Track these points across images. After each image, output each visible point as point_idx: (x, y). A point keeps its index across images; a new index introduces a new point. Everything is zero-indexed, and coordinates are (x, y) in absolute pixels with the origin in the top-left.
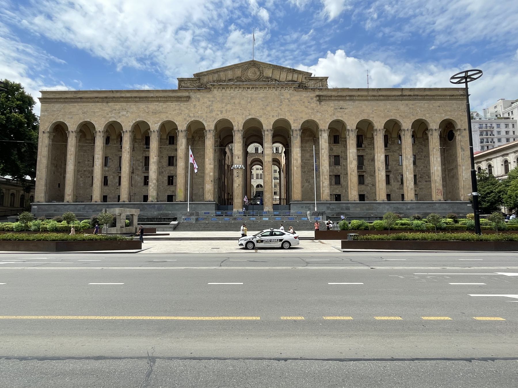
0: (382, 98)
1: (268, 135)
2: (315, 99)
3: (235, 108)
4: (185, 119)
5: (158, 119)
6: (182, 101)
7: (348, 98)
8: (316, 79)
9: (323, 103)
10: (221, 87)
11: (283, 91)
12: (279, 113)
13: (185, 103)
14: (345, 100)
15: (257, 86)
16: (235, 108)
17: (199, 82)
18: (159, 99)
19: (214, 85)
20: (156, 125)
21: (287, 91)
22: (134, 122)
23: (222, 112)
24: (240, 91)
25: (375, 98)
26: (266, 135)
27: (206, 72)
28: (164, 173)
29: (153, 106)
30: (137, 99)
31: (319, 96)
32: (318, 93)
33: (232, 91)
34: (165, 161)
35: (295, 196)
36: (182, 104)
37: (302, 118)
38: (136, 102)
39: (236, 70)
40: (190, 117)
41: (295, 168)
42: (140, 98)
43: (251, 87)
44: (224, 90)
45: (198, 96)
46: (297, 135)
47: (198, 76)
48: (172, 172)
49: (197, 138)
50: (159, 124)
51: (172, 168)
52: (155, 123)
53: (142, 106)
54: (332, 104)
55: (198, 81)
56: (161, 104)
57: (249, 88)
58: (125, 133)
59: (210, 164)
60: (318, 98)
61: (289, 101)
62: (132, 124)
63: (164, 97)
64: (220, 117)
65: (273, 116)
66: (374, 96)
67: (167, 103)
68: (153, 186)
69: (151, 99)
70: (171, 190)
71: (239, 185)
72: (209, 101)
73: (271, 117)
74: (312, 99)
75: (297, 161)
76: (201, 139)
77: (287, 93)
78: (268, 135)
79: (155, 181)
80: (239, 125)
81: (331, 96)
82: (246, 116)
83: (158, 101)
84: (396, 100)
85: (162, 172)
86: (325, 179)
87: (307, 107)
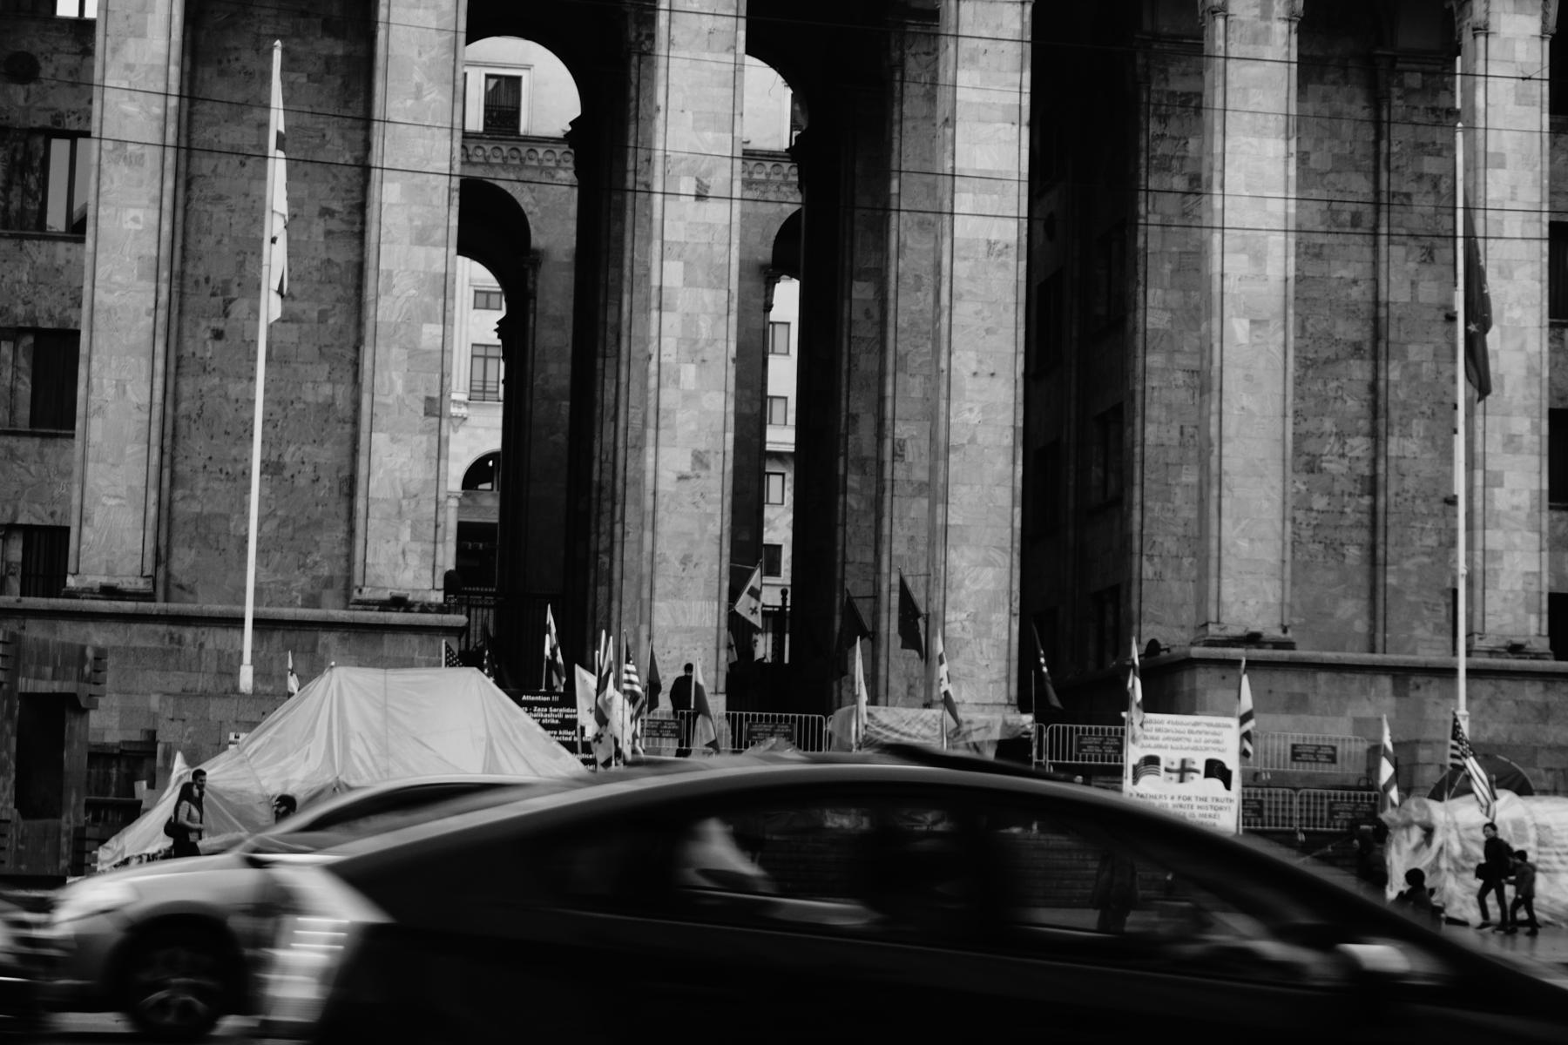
35: (1229, 591)
41: (1238, 329)
46: (1266, 15)
59: (422, 238)
71: (699, 459)
75: (1258, 258)
86: (1511, 443)
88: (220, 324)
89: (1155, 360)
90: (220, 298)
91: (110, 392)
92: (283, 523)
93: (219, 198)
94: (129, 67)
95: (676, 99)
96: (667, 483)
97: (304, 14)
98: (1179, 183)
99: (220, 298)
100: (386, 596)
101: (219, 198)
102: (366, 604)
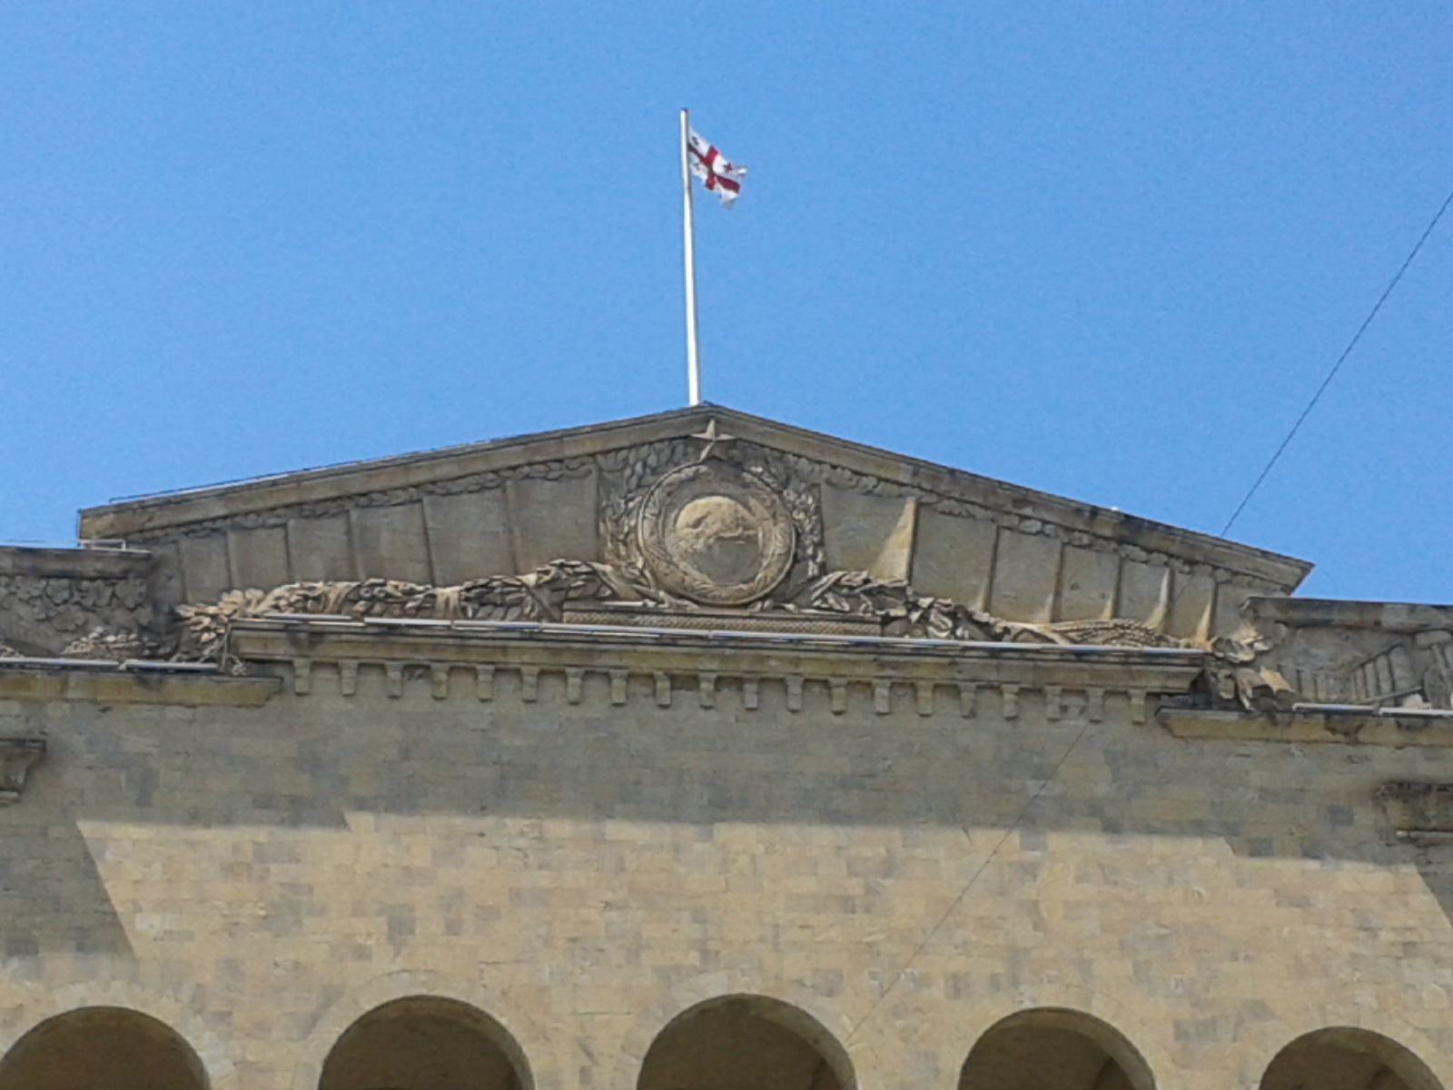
2: (1366, 817)
3: (544, 880)
8: (1354, 621)
11: (1037, 721)
12: (1015, 955)
15: (774, 667)
16: (544, 880)
17: (151, 600)
19: (317, 636)
21: (1075, 723)
24: (597, 708)
31: (1402, 789)
32: (1387, 758)
33: (509, 700)
37: (1260, 1010)
39: (543, 490)
43: (710, 666)
44: (418, 696)
55: (131, 590)
57: (692, 681)
60: (1396, 812)
64: (382, 980)
65: (958, 986)
73: (937, 992)
74: (1338, 815)
82: (669, 975)
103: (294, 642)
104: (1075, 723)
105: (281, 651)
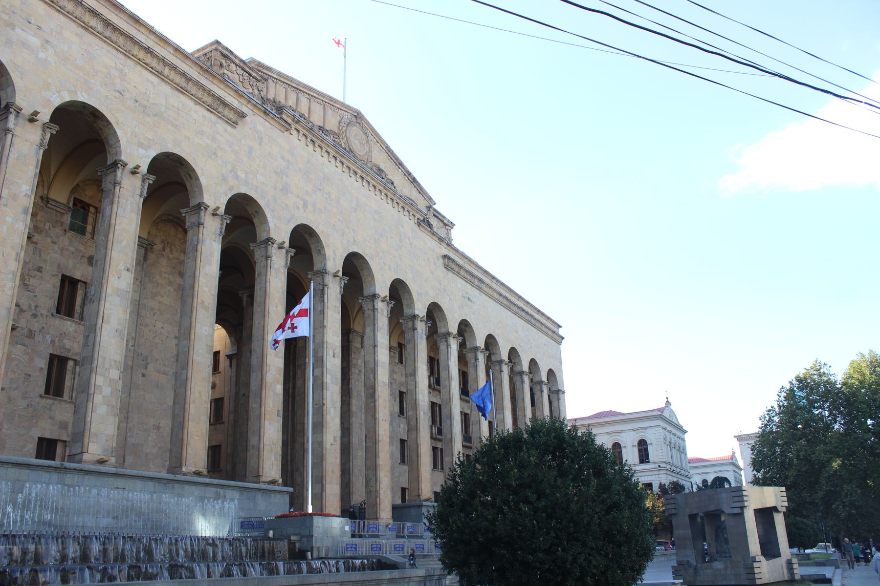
0: (505, 302)
1: (382, 310)
2: (441, 260)
4: (224, 179)
5: (150, 137)
6: (221, 117)
7: (476, 282)
9: (450, 275)
10: (310, 136)
13: (229, 128)
14: (472, 284)
18: (166, 71)
20: (142, 151)
22: (68, 99)
23: (305, 205)
25: (501, 299)
26: (379, 310)
27: (279, 74)
28: (39, 337)
29: (141, 80)
30: (93, 22)
34: (48, 290)
36: (221, 126)
38: (87, 28)
40: (237, 177)
41: (422, 413)
42: (107, 23)
45: (260, 128)
47: (258, 73)
48: (68, 343)
49: (158, 247)
50: (153, 154)
51: (69, 326)
52: (140, 145)
53: (106, 57)
54: (460, 283)
56: (166, 89)
57: (356, 173)
58: (21, 121)
61: (411, 244)
62: (57, 102)
63: (183, 74)
66: (500, 295)
67: (183, 98)
68: (107, 391)
69: (141, 55)
70: (59, 417)
71: (334, 438)
72: (283, 158)
76: (167, 250)
77: (408, 224)
78: (382, 310)
79: (115, 374)
80: (337, 260)
81: (460, 267)
83: (159, 74)
84: (515, 313)
85: (31, 334)
87: (432, 273)
88: (143, 371)
89: (354, 419)
90: (144, 363)
91: (197, 394)
92: (160, 448)
93: (146, 325)
94: (206, 274)
95: (329, 326)
96: (328, 446)
97: (174, 268)
98: (357, 371)
99: (144, 363)
100: (270, 479)
101: (146, 325)
102: (264, 482)
103: (293, 120)
104: (407, 218)
105: (290, 121)
